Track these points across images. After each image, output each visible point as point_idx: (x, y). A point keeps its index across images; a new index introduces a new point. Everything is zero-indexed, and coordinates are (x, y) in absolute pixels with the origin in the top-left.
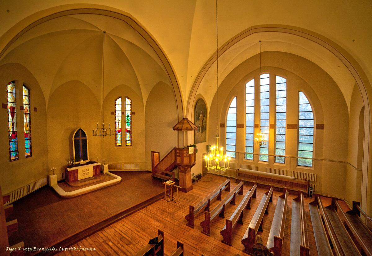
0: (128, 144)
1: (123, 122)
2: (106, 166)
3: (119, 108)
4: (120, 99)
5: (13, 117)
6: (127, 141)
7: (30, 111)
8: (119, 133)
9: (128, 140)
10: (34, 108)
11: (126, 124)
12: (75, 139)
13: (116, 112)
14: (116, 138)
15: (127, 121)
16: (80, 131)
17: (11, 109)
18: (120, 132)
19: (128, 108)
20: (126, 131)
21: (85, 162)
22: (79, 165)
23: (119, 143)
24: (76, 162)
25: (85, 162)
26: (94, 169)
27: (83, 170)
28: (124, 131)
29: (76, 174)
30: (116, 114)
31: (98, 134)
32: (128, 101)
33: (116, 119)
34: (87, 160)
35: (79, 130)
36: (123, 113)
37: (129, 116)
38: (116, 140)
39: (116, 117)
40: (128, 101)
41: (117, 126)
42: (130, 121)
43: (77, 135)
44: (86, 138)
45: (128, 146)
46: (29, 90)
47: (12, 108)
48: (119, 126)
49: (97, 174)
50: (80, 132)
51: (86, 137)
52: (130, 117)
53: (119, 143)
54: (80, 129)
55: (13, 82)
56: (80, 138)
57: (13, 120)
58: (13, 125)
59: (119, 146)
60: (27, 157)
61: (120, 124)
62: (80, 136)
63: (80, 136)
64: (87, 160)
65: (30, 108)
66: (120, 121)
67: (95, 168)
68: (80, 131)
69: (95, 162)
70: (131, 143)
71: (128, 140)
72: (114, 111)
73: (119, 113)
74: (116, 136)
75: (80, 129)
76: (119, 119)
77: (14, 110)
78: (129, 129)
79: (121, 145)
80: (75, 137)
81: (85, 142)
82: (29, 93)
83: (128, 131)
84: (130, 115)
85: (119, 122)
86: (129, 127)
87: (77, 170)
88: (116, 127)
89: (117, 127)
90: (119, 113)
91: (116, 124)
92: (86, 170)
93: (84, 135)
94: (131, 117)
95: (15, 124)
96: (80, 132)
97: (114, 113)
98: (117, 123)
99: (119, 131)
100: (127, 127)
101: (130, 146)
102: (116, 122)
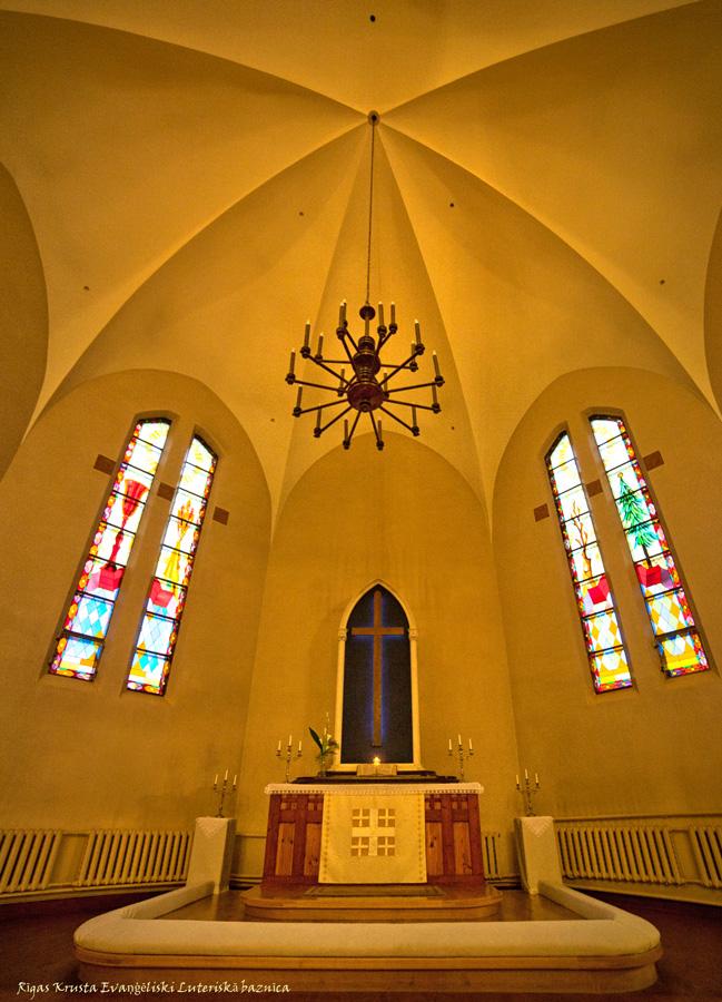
0: (679, 658)
1: (611, 536)
2: (538, 830)
4: (565, 439)
5: (128, 512)
6: (668, 645)
7: (202, 518)
8: (602, 606)
9: (672, 636)
10: (216, 508)
11: (631, 538)
12: (349, 634)
13: (558, 504)
14: (588, 642)
15: (626, 525)
16: (378, 594)
17: (129, 487)
18: (605, 599)
20: (640, 582)
21: (391, 769)
24: (343, 761)
25: (391, 769)
26: (431, 818)
27: (356, 812)
28: (623, 581)
29: (310, 827)
30: (560, 514)
31: (297, 379)
33: (565, 538)
34: (411, 761)
35: (369, 595)
37: (631, 493)
38: (592, 656)
39: (563, 528)
41: (579, 565)
42: (645, 511)
43: (360, 614)
44: (407, 633)
45: (683, 672)
46: (216, 457)
47: (136, 489)
48: (589, 564)
49: (459, 870)
51: (406, 625)
52: (639, 495)
53: (613, 669)
54: (379, 587)
57: (124, 522)
58: (119, 537)
59: (618, 688)
60: (143, 690)
61: (593, 552)
62: (377, 617)
63: (377, 617)
64: (410, 760)
65: (204, 508)
66: (592, 538)
68: (378, 594)
69: (452, 780)
70: (704, 648)
71: (672, 636)
72: (547, 500)
73: (574, 501)
74: (585, 630)
75: (379, 587)
76: (581, 531)
77: (139, 495)
78: (663, 564)
79: (626, 676)
80: (349, 626)
82: (215, 467)
83: (655, 576)
84: (634, 484)
85: (585, 546)
86: (655, 548)
87: (319, 799)
88: (574, 575)
89: (580, 577)
90: (574, 501)
91: (570, 559)
92: (374, 818)
93: (395, 614)
94: (645, 491)
95: (127, 541)
97: (549, 511)
98: (577, 556)
99: (597, 596)
100: (638, 555)
101: (701, 669)
102: (569, 551)
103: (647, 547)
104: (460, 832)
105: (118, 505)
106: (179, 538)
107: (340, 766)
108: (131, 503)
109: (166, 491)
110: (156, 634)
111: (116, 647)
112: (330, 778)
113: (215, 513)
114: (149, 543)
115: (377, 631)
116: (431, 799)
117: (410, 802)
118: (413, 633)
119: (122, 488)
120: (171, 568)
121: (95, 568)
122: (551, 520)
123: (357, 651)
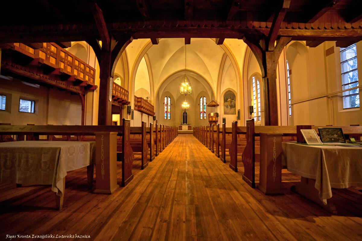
1: (203, 108)
3: (201, 102)
19: (205, 101)
22: (184, 125)
23: (201, 118)
32: (205, 98)
36: (203, 104)
40: (205, 98)
41: (201, 110)
47: (166, 104)
48: (201, 110)
50: (185, 113)
53: (201, 118)
55: (166, 97)
56: (185, 115)
67: (188, 127)
76: (201, 107)
78: (205, 112)
81: (186, 116)
83: (205, 112)
90: (201, 104)
93: (186, 114)
96: (185, 113)
97: (199, 104)
103: (205, 110)
104: (190, 128)
105: (165, 106)
106: (169, 107)
107: (183, 124)
108: (166, 105)
109: (168, 104)
110: (169, 115)
111: (167, 117)
112: (183, 125)
113: (171, 104)
114: (167, 109)
115: (185, 115)
116: (188, 126)
117: (187, 126)
118: (188, 115)
119: (165, 105)
120: (169, 110)
121: (165, 112)
122: (199, 105)
123: (184, 116)
